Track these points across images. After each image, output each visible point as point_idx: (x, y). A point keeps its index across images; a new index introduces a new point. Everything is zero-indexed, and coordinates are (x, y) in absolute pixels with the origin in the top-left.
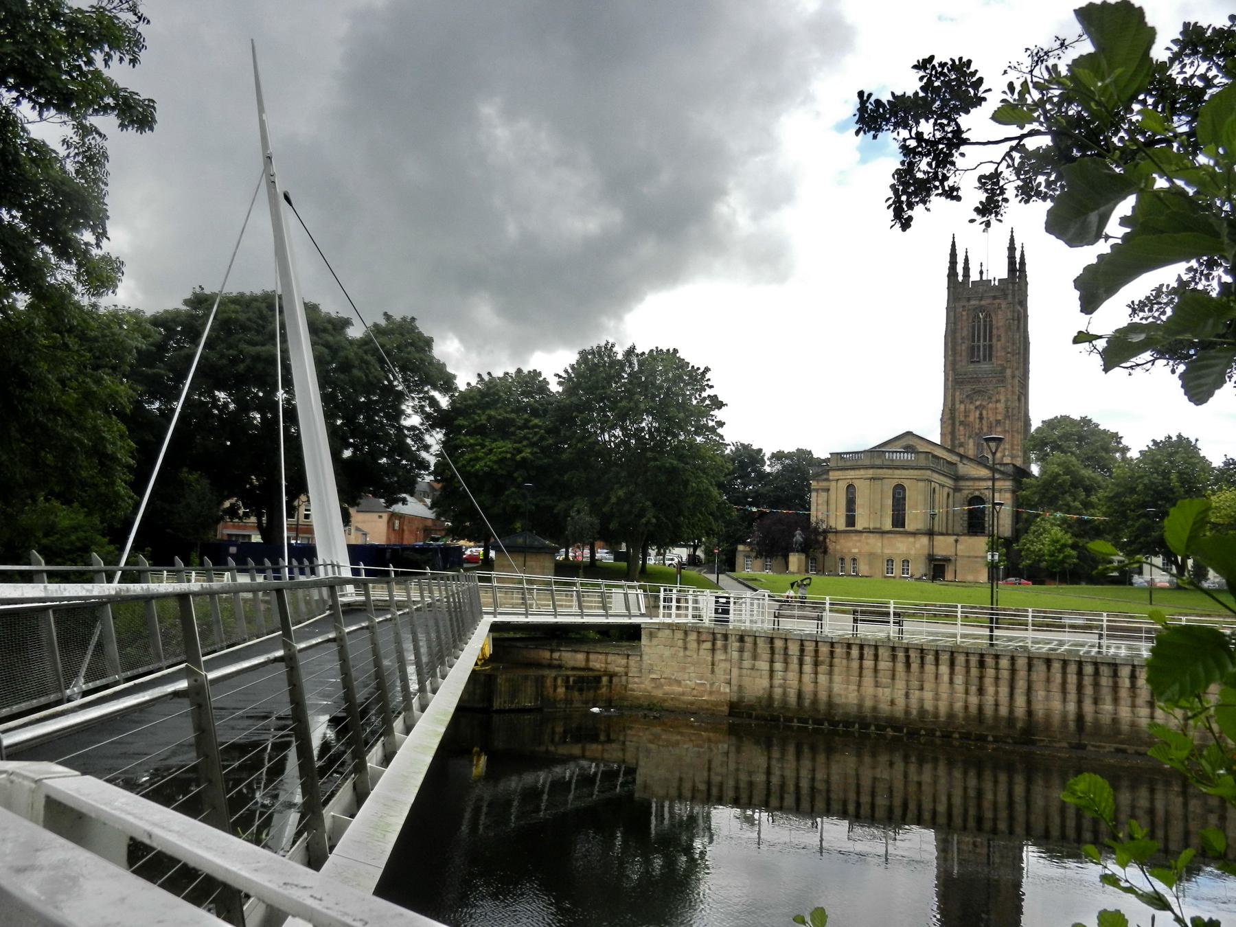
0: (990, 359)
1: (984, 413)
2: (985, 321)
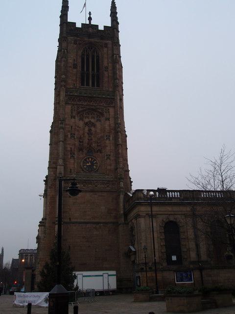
0: (98, 86)
1: (93, 129)
2: (93, 56)
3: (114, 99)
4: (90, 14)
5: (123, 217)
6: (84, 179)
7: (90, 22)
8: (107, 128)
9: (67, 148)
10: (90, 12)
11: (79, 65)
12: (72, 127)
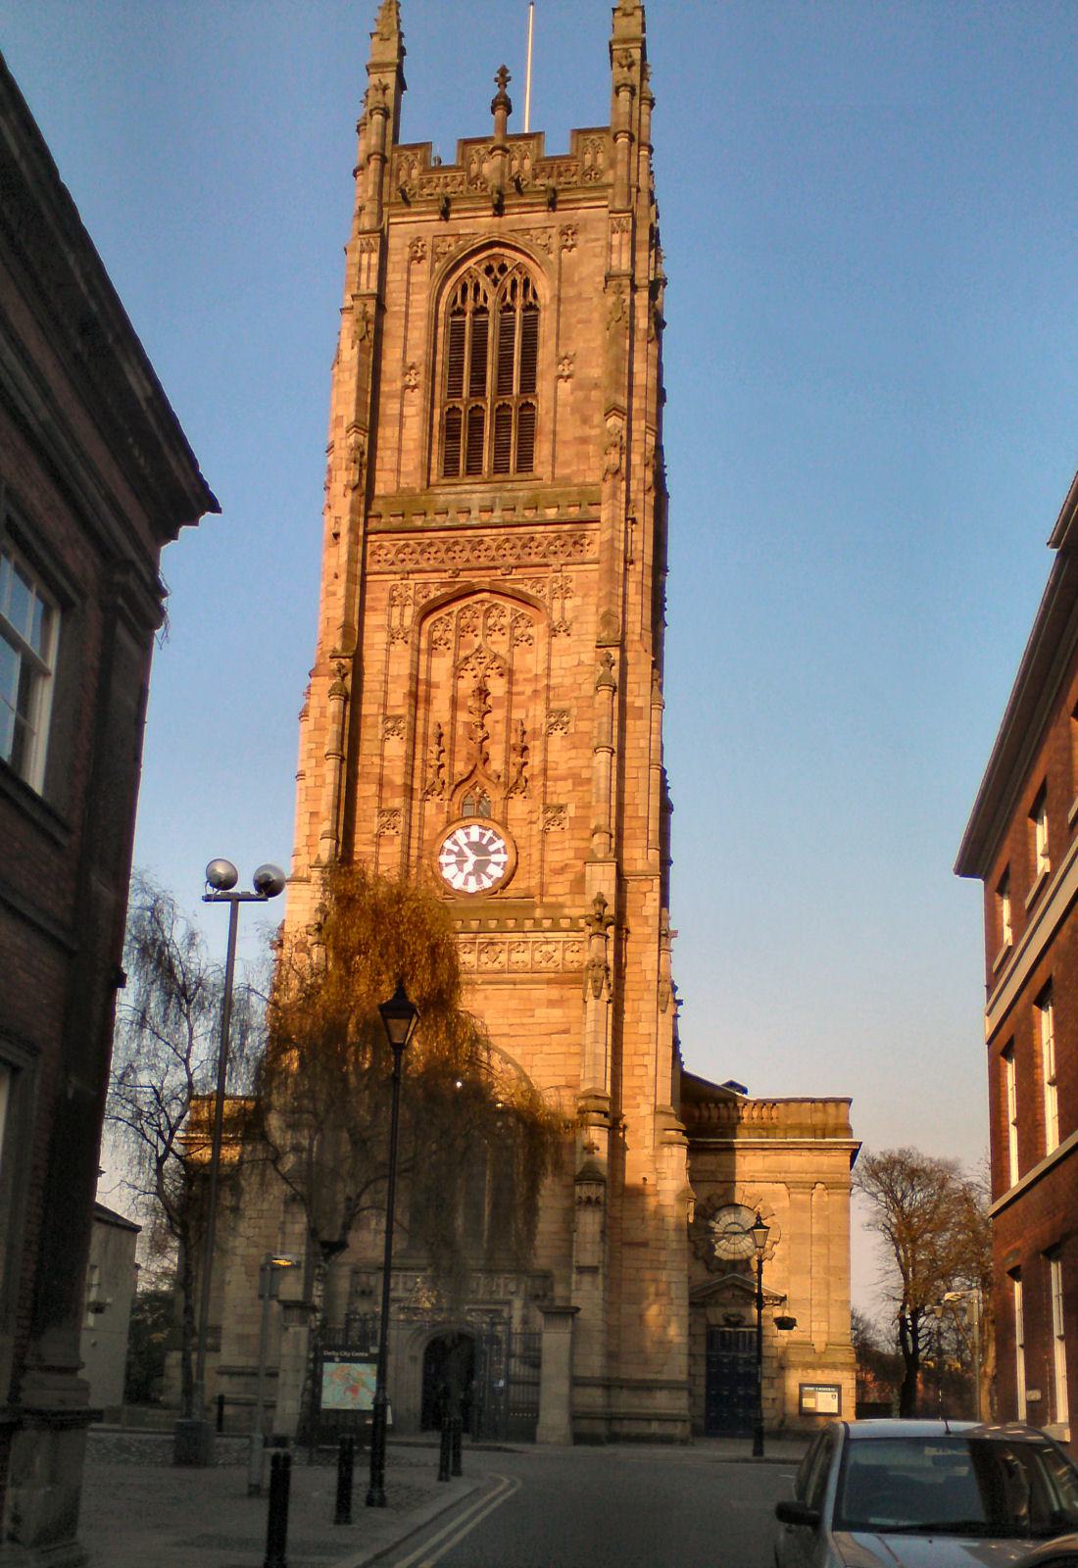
0: (526, 461)
1: (497, 687)
4: (503, 77)
10: (503, 71)
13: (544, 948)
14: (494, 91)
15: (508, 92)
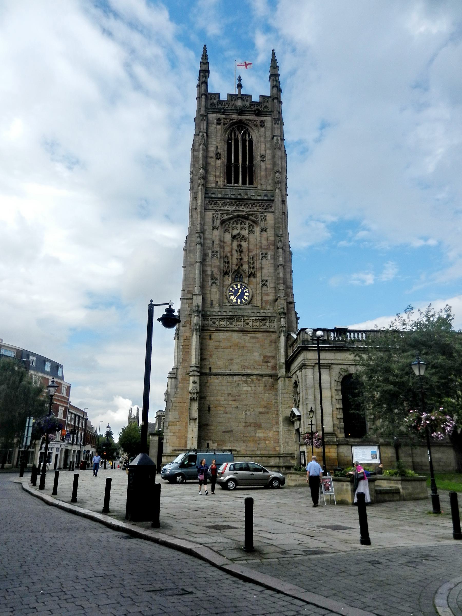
0: (251, 183)
1: (244, 244)
2: (244, 141)
3: (273, 200)
5: (284, 367)
6: (231, 314)
7: (240, 91)
8: (264, 242)
9: (206, 271)
10: (240, 77)
11: (224, 154)
12: (213, 242)
13: (263, 322)
14: (238, 82)
15: (242, 82)
